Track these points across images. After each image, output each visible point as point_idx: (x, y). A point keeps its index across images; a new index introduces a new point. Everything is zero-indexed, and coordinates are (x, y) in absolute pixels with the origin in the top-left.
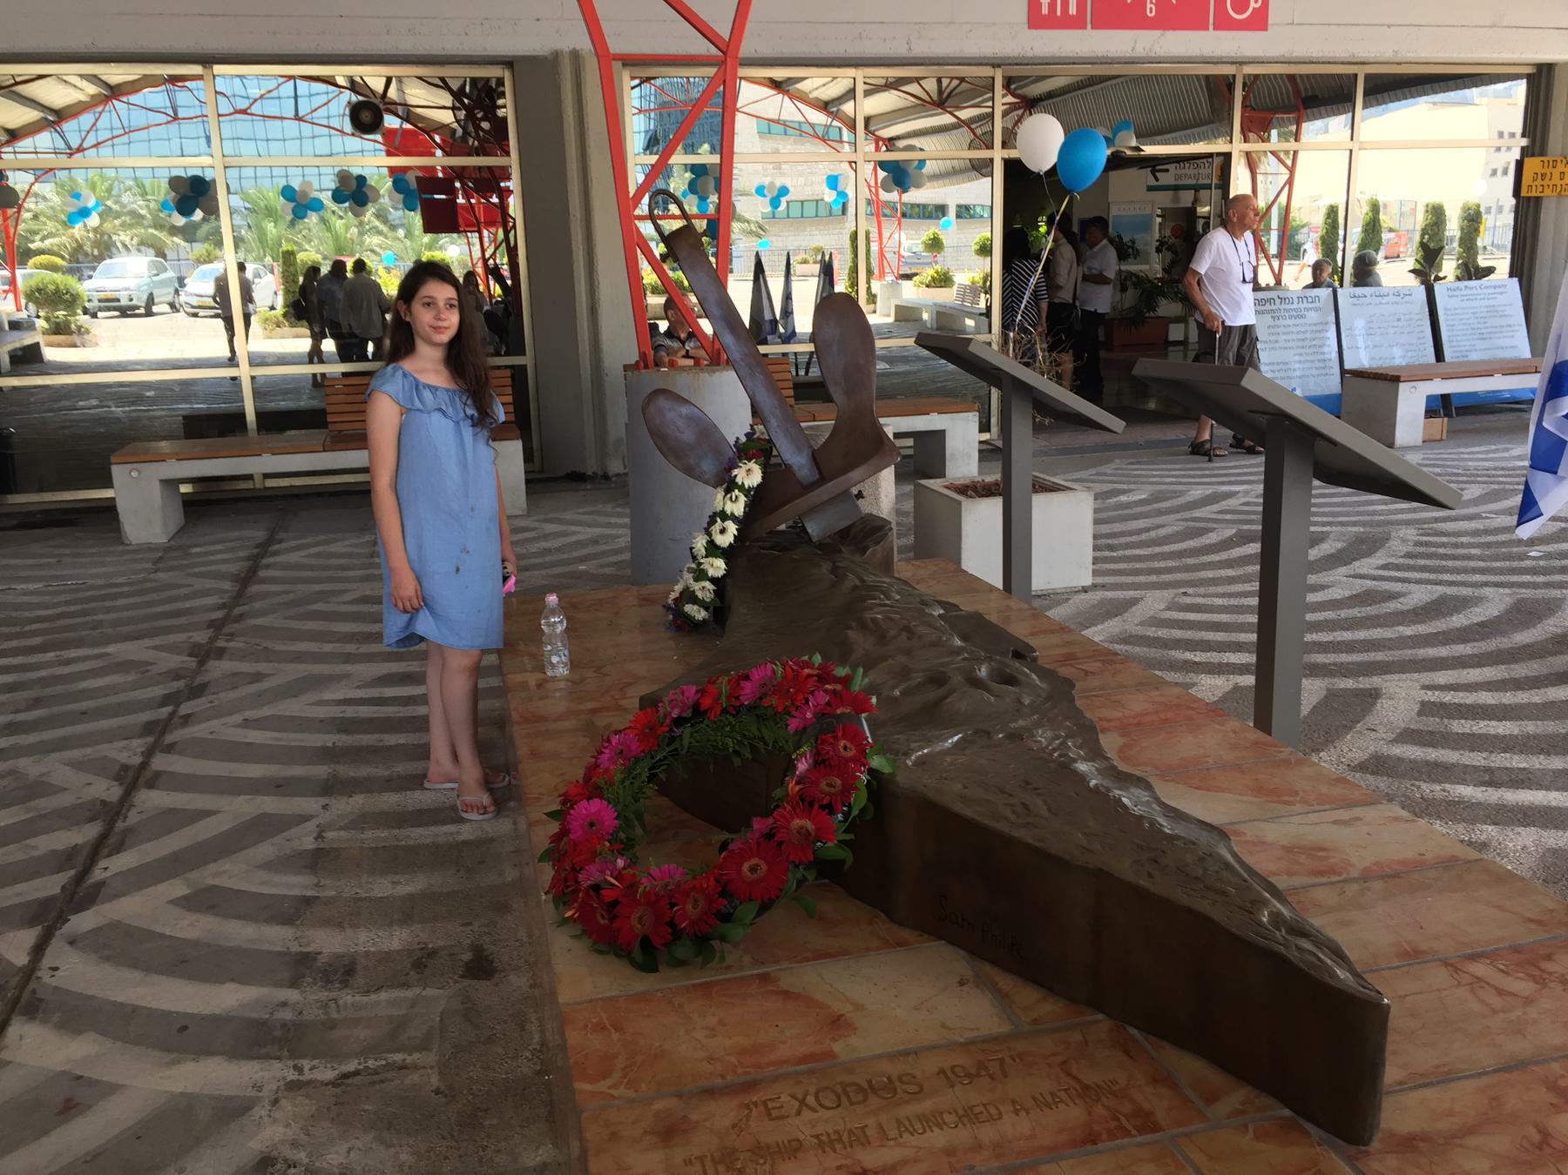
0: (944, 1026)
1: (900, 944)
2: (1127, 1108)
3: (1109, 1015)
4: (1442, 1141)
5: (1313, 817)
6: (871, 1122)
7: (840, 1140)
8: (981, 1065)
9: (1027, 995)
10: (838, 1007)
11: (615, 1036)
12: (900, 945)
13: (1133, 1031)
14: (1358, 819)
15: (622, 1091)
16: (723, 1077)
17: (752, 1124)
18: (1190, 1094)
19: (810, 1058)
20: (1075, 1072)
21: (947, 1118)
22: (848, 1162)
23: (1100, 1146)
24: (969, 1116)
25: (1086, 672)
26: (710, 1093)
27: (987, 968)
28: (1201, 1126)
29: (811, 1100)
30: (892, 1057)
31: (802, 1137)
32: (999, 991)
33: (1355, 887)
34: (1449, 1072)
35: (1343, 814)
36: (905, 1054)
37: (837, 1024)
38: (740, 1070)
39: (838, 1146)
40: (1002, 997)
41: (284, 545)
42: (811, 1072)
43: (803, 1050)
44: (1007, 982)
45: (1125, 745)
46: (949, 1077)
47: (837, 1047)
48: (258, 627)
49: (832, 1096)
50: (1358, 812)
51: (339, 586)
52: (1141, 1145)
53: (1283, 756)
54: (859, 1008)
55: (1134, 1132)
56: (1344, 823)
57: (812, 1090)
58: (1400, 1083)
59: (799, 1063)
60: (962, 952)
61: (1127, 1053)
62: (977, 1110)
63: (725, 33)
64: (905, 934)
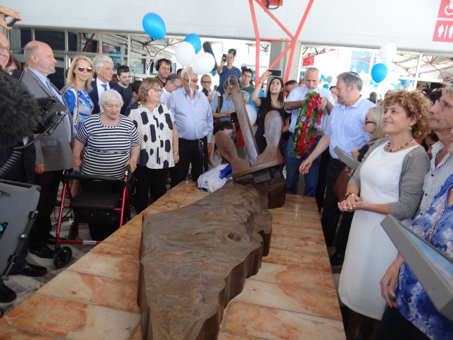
1: (130, 310)
5: (308, 317)
10: (88, 322)
14: (323, 323)
25: (306, 244)
27: (140, 328)
35: (320, 320)
44: (139, 334)
45: (285, 272)
50: (327, 321)
53: (328, 291)
54: (93, 324)
56: (316, 323)
63: (294, 34)
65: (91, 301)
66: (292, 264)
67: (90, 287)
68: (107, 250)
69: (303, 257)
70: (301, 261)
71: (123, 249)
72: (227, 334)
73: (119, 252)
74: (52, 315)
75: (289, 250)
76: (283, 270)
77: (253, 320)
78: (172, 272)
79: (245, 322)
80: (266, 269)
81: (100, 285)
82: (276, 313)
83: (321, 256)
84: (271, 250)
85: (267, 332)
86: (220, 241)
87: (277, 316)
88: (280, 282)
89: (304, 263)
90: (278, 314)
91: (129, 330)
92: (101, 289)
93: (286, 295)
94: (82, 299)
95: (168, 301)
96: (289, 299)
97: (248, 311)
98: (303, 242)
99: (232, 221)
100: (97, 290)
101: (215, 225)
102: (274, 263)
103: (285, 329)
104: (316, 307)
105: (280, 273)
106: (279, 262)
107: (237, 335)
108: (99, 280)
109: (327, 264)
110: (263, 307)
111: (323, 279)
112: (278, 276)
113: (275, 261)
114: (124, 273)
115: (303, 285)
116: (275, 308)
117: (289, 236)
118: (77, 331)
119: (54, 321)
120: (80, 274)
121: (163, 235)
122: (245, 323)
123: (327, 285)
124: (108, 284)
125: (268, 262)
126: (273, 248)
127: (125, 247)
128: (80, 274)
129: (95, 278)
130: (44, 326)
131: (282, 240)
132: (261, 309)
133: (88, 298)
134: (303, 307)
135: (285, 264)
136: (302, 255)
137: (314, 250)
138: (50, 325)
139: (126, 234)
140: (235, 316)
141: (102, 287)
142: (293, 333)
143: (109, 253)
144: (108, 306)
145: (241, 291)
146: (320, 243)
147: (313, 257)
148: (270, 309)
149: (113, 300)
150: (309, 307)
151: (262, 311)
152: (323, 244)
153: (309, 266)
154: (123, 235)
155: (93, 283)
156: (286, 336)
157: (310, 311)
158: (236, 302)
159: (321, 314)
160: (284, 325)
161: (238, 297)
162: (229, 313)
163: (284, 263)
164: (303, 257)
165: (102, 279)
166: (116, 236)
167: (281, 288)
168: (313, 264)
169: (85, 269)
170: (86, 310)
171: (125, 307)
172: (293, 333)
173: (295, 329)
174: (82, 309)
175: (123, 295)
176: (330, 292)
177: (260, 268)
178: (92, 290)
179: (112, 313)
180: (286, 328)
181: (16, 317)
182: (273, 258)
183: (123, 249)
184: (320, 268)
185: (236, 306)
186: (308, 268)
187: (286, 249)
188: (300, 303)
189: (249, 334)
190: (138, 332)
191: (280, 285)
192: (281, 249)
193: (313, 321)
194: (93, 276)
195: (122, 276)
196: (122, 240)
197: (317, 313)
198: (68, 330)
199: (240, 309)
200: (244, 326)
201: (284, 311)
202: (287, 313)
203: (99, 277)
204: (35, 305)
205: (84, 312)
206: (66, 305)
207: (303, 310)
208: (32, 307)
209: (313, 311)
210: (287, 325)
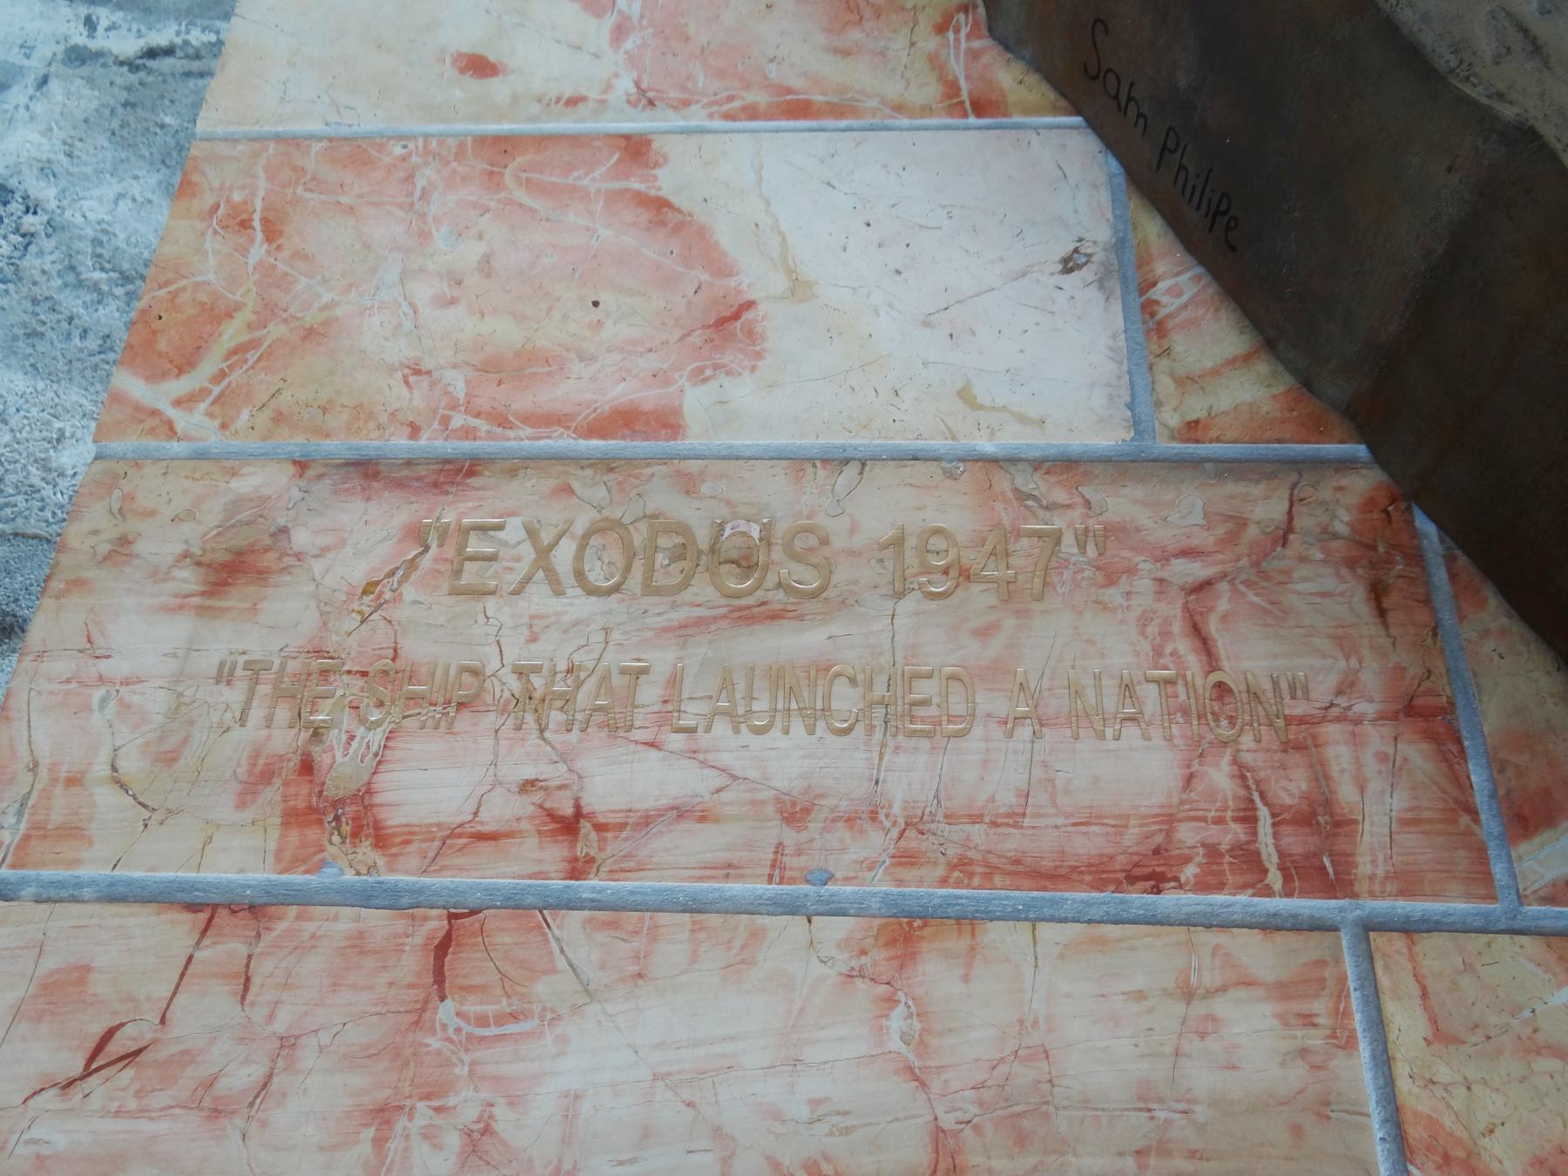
0: (965, 395)
1: (984, 106)
2: (1292, 787)
3: (1380, 457)
6: (662, 659)
7: (567, 700)
9: (1212, 337)
10: (757, 278)
11: (258, 251)
12: (980, 107)
13: (1426, 526)
15: (196, 423)
16: (415, 430)
17: (409, 593)
18: (1478, 777)
19: (624, 420)
20: (1213, 627)
21: (845, 700)
22: (553, 773)
23: (1170, 900)
24: (898, 710)
26: (367, 472)
27: (1153, 229)
28: (1459, 907)
29: (564, 555)
30: (799, 462)
31: (493, 665)
32: (1149, 308)
36: (837, 461)
37: (729, 325)
38: (458, 420)
39: (556, 717)
40: (1152, 326)
42: (606, 464)
43: (618, 393)
44: (1180, 283)
46: (912, 566)
47: (695, 401)
49: (615, 555)
52: (1270, 926)
54: (799, 288)
55: (1275, 878)
57: (580, 526)
59: (596, 429)
60: (1114, 165)
61: (1377, 592)
62: (924, 689)
64: (1009, 77)
65: (646, 99)
91: (1087, 274)
94: (573, 102)
119: (504, 332)
133: (609, 87)
138: (495, 366)
174: (636, 185)
181: (209, 365)
190: (1161, 267)
206: (493, 179)
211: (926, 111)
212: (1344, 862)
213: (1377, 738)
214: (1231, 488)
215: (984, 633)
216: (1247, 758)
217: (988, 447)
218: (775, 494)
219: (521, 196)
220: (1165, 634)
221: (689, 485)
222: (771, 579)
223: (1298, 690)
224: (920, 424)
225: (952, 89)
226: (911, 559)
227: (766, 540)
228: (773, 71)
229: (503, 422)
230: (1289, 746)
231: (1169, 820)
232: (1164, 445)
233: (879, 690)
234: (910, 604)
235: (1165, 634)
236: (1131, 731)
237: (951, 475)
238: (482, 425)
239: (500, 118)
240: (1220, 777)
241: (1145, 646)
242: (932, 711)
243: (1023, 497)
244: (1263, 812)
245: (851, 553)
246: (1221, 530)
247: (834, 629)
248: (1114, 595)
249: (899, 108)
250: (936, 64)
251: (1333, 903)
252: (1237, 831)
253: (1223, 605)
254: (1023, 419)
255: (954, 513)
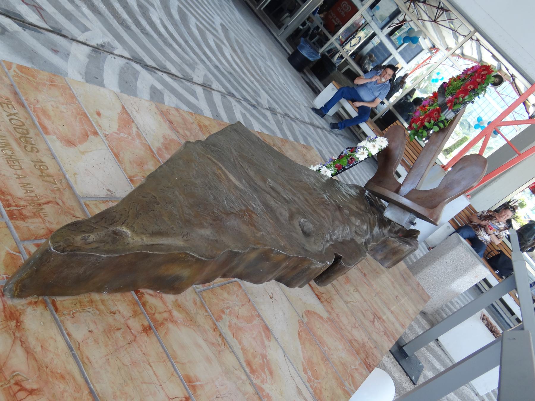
0: (75, 174)
4: (17, 334)
5: (298, 379)
8: (49, 176)
10: (82, 147)
12: (131, 180)
19: (44, 128)
25: (373, 322)
30: (49, 150)
32: (107, 201)
33: (244, 377)
34: (83, 362)
40: (105, 201)
41: (336, 137)
45: (321, 318)
48: (291, 125)
51: (323, 146)
53: (346, 383)
54: (83, 153)
56: (300, 392)
58: (69, 334)
59: (40, 124)
66: (336, 319)
67: (119, 126)
68: (171, 118)
69: (355, 327)
70: (349, 328)
71: (188, 133)
72: (198, 299)
73: (181, 131)
74: (57, 108)
75: (347, 307)
76: (321, 315)
77: (237, 317)
78: (207, 182)
79: (228, 310)
80: (304, 295)
81: (129, 134)
82: (268, 338)
83: (376, 348)
84: (329, 286)
85: (240, 343)
86: (287, 215)
87: (266, 342)
88: (306, 320)
89: (351, 334)
90: (270, 341)
91: (109, 193)
92: (126, 138)
93: (297, 336)
94: (99, 126)
95: (171, 196)
96: (298, 343)
97: (242, 305)
98: (372, 317)
99: (320, 214)
100: (122, 135)
101: (299, 198)
102: (319, 299)
103: (261, 361)
104: (316, 381)
105: (315, 313)
106: (325, 303)
107: (207, 311)
108: (134, 130)
109: (373, 360)
110: (262, 319)
111: (353, 367)
112: (309, 313)
113: (322, 299)
114: (164, 150)
115: (326, 348)
116: (272, 334)
117: (362, 297)
118: (61, 142)
119: (52, 113)
120: (123, 107)
121: (236, 152)
122: (227, 311)
123: (352, 376)
124: (138, 141)
125: (314, 292)
126: (334, 286)
127: (191, 133)
128: (123, 107)
129: (133, 125)
130: (38, 106)
131: (352, 291)
132: (257, 319)
134: (303, 365)
135: (330, 313)
136: (357, 325)
137: (375, 336)
138: (45, 112)
139: (206, 126)
140: (225, 295)
141: (130, 138)
142: (265, 373)
143: (171, 122)
144: (116, 156)
145: (257, 284)
146: (388, 337)
147: (366, 339)
148: (267, 329)
149: (127, 156)
150: (309, 373)
151: (257, 321)
152: (391, 342)
153: (353, 341)
154: (201, 124)
155: (126, 126)
156: (254, 368)
157: (305, 375)
158: (240, 287)
159: (315, 391)
160: (263, 356)
161: (247, 284)
162: (222, 286)
163: (330, 310)
164: (355, 327)
165: (137, 132)
166: (194, 117)
167: (300, 326)
168: (359, 344)
169: (133, 109)
170: (92, 137)
171: (131, 174)
172: (265, 373)
173: (271, 373)
174: (89, 133)
175: (141, 164)
176: (348, 385)
177: (300, 287)
178: (118, 130)
179: (111, 165)
180: (264, 362)
181: (23, 75)
182: (323, 295)
183: (188, 133)
184: (363, 355)
185: (236, 289)
186: (350, 341)
187: (346, 302)
188: (304, 359)
189: (220, 324)
191: (301, 322)
192: (341, 297)
193: (298, 388)
194: (133, 122)
195: (159, 149)
196: (195, 126)
197: (311, 387)
198: (55, 133)
199: (237, 296)
200: (223, 312)
201: (279, 346)
202: (280, 352)
203: (138, 128)
204: (53, 85)
205: (88, 136)
206: (79, 114)
207: (301, 368)
208: (48, 83)
209: (309, 381)
210: (268, 361)
211: (127, 173)
212: (16, 219)
213: (42, 226)
214: (79, 210)
215: (31, 172)
216: (28, 207)
217: (67, 176)
218: (41, 146)
219: (78, 118)
220: (45, 198)
221: (37, 135)
222: (26, 145)
223: (46, 216)
224: (66, 167)
225: (134, 177)
226: (40, 164)
227: (32, 144)
228: (121, 153)
229: (35, 111)
230: (34, 213)
231: (11, 195)
232: (82, 201)
233: (13, 157)
234: (33, 164)
235: (45, 198)
236: (25, 191)
237: (59, 170)
238: (32, 108)
239: (89, 113)
240: (22, 203)
241: (42, 194)
242: (13, 164)
243: (61, 180)
244: (20, 208)
245: (36, 155)
246: (70, 207)
247: (21, 152)
248: (49, 191)
249: (125, 170)
250: (137, 175)
251: (7, 217)
252: (14, 204)
253: (56, 206)
254: (75, 181)
255: (52, 170)
